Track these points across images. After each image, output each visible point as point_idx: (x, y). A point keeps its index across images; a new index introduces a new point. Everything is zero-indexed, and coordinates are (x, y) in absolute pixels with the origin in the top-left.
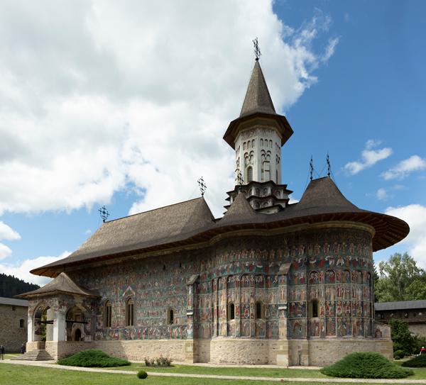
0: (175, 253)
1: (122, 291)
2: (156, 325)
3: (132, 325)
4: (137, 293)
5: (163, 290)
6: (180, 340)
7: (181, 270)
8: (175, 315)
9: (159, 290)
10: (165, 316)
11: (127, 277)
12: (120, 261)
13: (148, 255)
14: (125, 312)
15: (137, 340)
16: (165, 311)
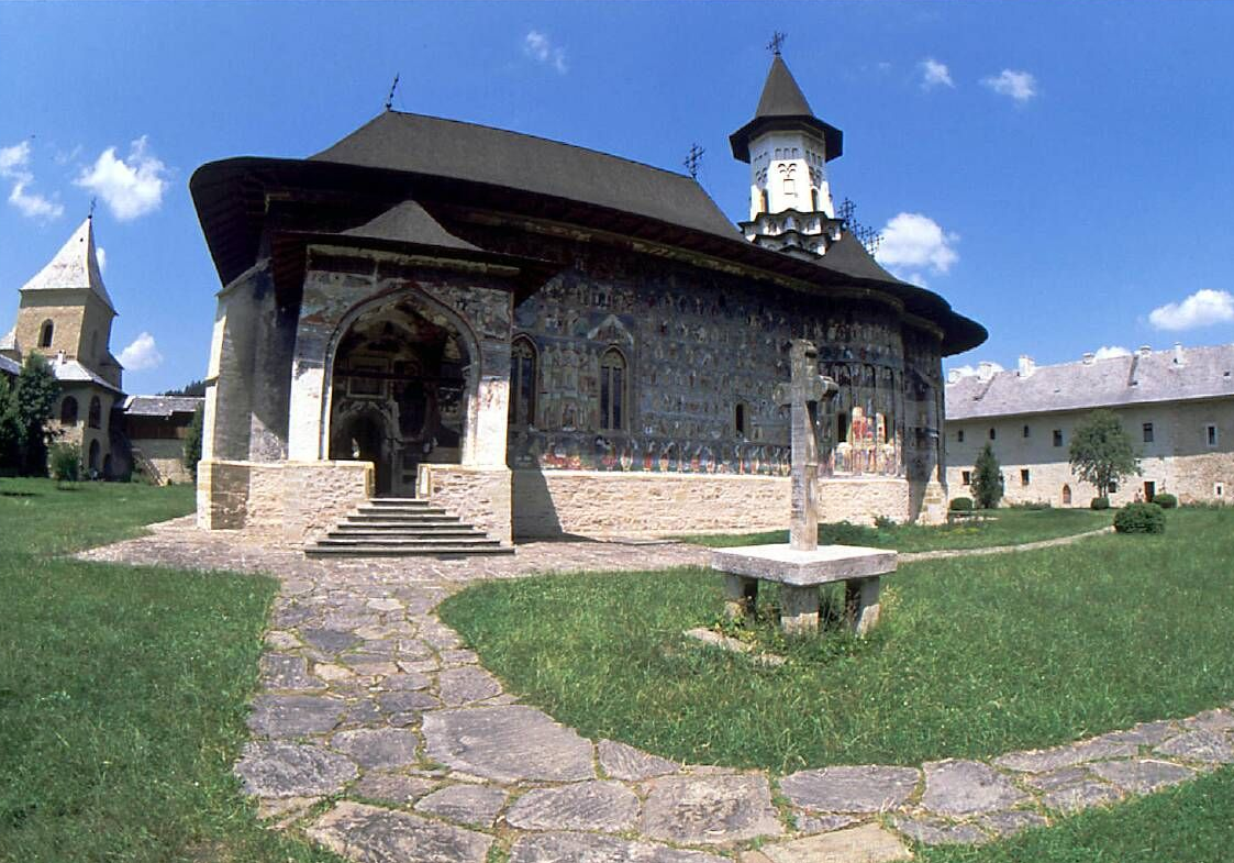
0: (747, 279)
1: (585, 321)
2: (703, 436)
3: (617, 425)
4: (638, 339)
5: (721, 353)
6: (765, 477)
7: (762, 321)
8: (751, 419)
9: (710, 350)
10: (730, 416)
11: (607, 289)
12: (581, 237)
13: (680, 257)
14: (598, 387)
15: (640, 474)
16: (726, 405)
